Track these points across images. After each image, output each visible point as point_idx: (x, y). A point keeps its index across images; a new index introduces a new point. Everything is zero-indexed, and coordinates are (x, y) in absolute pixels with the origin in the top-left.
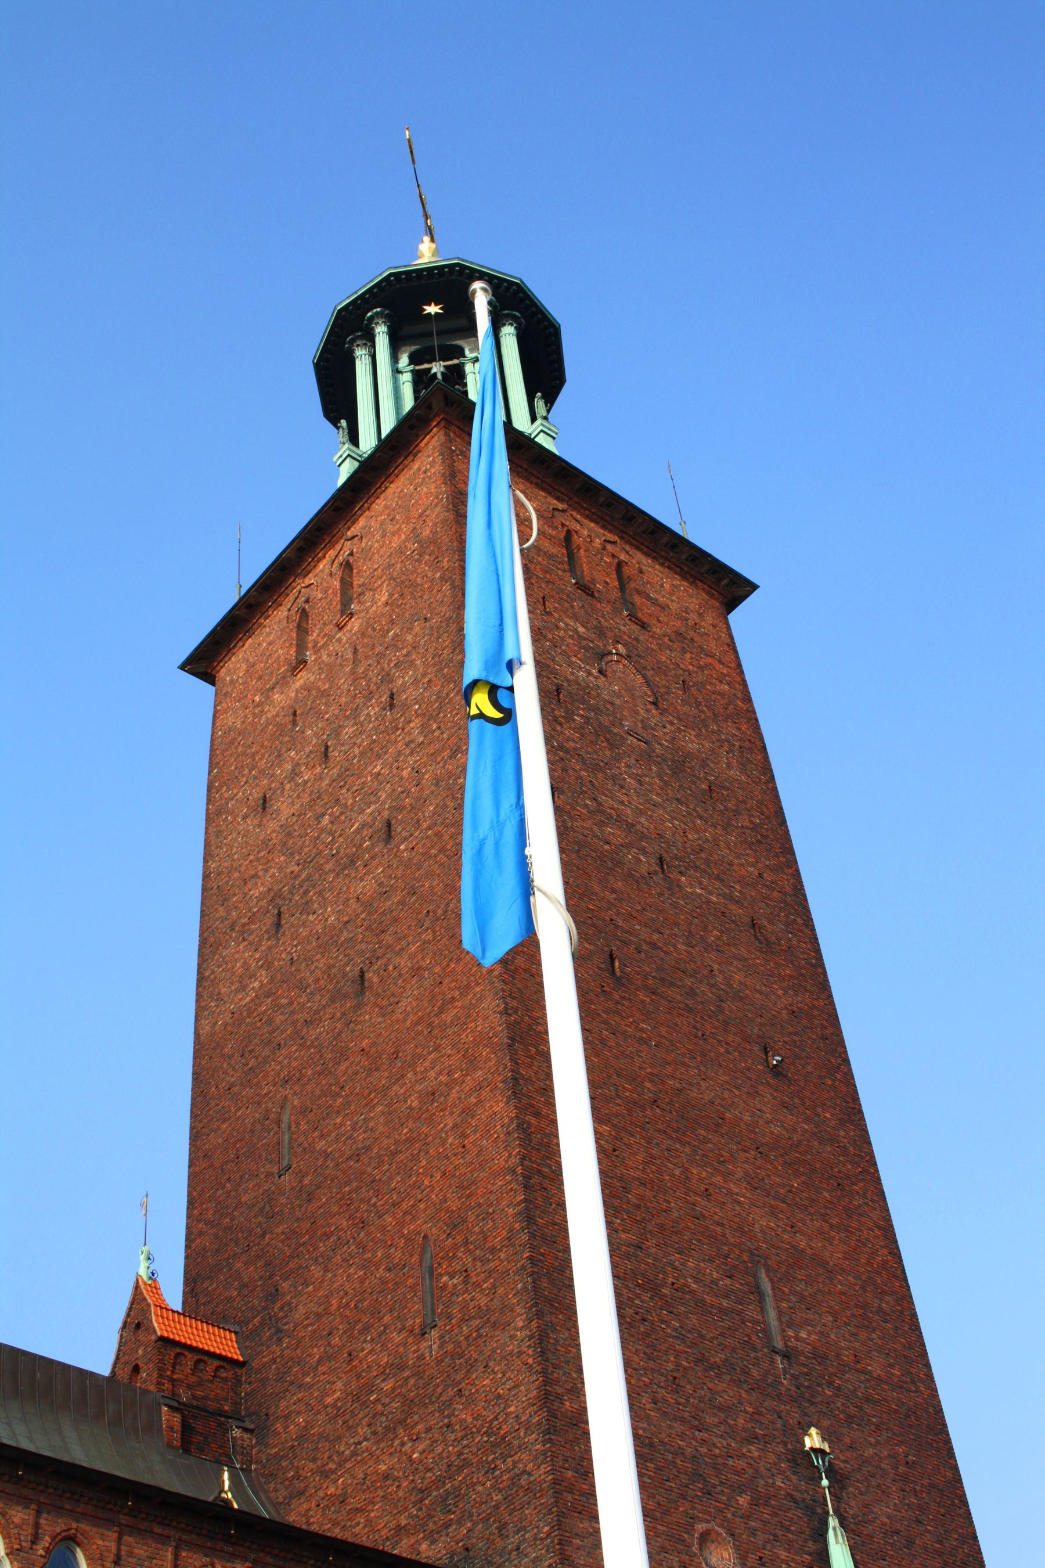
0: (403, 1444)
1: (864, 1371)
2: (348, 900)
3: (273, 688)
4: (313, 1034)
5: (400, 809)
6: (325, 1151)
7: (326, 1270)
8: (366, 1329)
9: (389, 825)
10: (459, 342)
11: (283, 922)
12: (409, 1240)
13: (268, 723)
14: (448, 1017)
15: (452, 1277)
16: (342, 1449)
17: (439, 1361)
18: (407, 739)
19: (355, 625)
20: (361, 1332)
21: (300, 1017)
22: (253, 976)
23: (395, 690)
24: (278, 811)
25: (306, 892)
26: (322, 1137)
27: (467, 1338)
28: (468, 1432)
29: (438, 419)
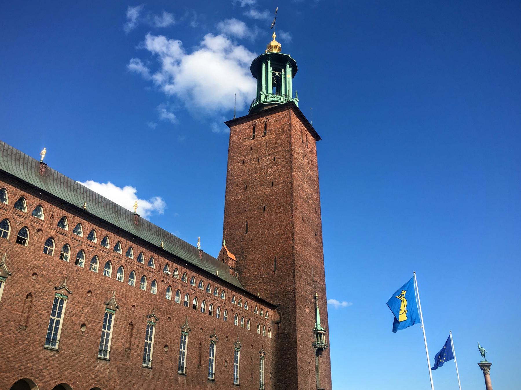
0: (269, 286)
1: (320, 283)
2: (262, 192)
7: (254, 253)
9: (272, 183)
16: (257, 282)
18: (277, 169)
19: (267, 138)
20: (261, 266)
27: (282, 275)
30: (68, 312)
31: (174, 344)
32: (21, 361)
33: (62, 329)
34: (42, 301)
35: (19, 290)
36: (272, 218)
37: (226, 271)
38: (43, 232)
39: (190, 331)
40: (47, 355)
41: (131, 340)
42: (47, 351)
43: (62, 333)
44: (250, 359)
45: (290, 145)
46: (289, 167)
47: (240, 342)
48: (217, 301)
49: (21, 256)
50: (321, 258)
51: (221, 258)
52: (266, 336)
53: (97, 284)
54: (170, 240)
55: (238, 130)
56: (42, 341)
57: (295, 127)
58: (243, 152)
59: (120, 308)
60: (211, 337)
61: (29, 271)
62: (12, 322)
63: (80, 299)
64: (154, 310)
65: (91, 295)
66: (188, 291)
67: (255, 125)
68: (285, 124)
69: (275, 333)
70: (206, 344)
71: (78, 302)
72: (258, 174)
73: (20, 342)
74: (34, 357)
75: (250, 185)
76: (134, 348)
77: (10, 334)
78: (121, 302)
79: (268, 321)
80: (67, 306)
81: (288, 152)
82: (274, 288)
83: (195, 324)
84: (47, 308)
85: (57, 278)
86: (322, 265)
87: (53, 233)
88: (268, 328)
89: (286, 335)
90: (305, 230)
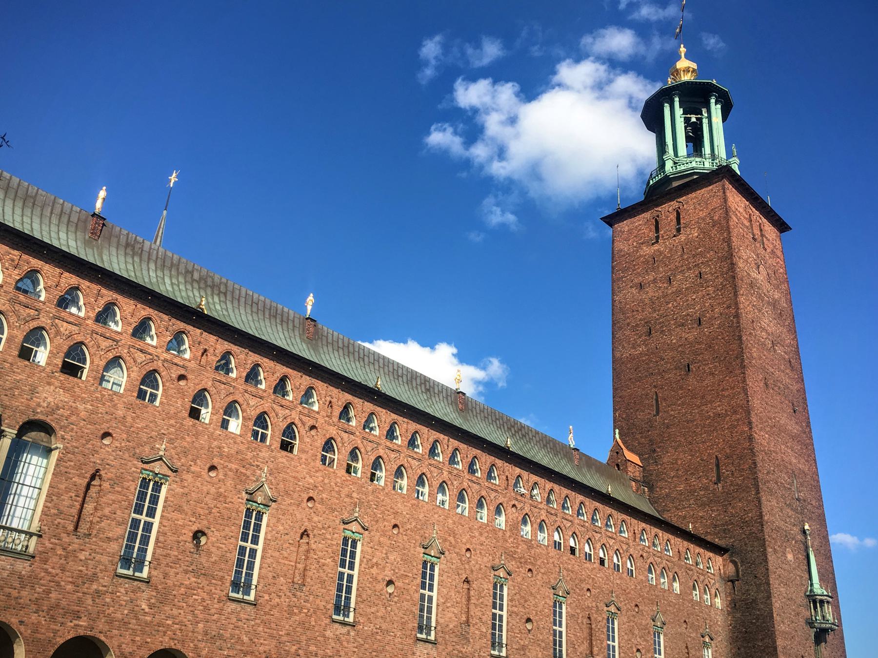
0: (708, 511)
1: (812, 504)
2: (681, 337)
4: (667, 376)
8: (692, 474)
13: (641, 256)
14: (726, 394)
15: (727, 471)
16: (684, 504)
17: (722, 493)
19: (682, 237)
20: (691, 474)
21: (662, 369)
22: (639, 346)
24: (648, 292)
25: (662, 327)
26: (672, 410)
30: (365, 560)
31: (541, 617)
32: (299, 642)
33: (358, 589)
34: (324, 542)
35: (289, 525)
36: (704, 384)
37: (623, 485)
38: (319, 430)
39: (569, 594)
40: (338, 633)
41: (468, 608)
42: (337, 625)
43: (358, 596)
44: (684, 647)
45: (730, 246)
46: (730, 286)
47: (663, 615)
48: (613, 541)
49: (288, 471)
50: (809, 456)
51: (613, 462)
52: (711, 606)
53: (407, 514)
54: (520, 433)
55: (626, 229)
56: (329, 609)
57: (737, 212)
58: (638, 268)
59: (447, 553)
60: (607, 606)
61: (302, 494)
62: (282, 578)
63: (381, 539)
64: (503, 558)
65: (399, 533)
66: (558, 524)
67: (658, 216)
68: (715, 208)
69: (729, 599)
70: (600, 619)
71: (380, 543)
72: (670, 305)
73: (295, 611)
74: (318, 636)
75: (658, 327)
76: (474, 622)
77: (280, 597)
78: (448, 543)
79: (712, 577)
80: (362, 551)
81: (726, 259)
82: (719, 515)
83: (577, 581)
84: (332, 555)
85: (345, 504)
86: (813, 469)
87: (333, 431)
88: (713, 591)
89: (751, 603)
90: (771, 403)
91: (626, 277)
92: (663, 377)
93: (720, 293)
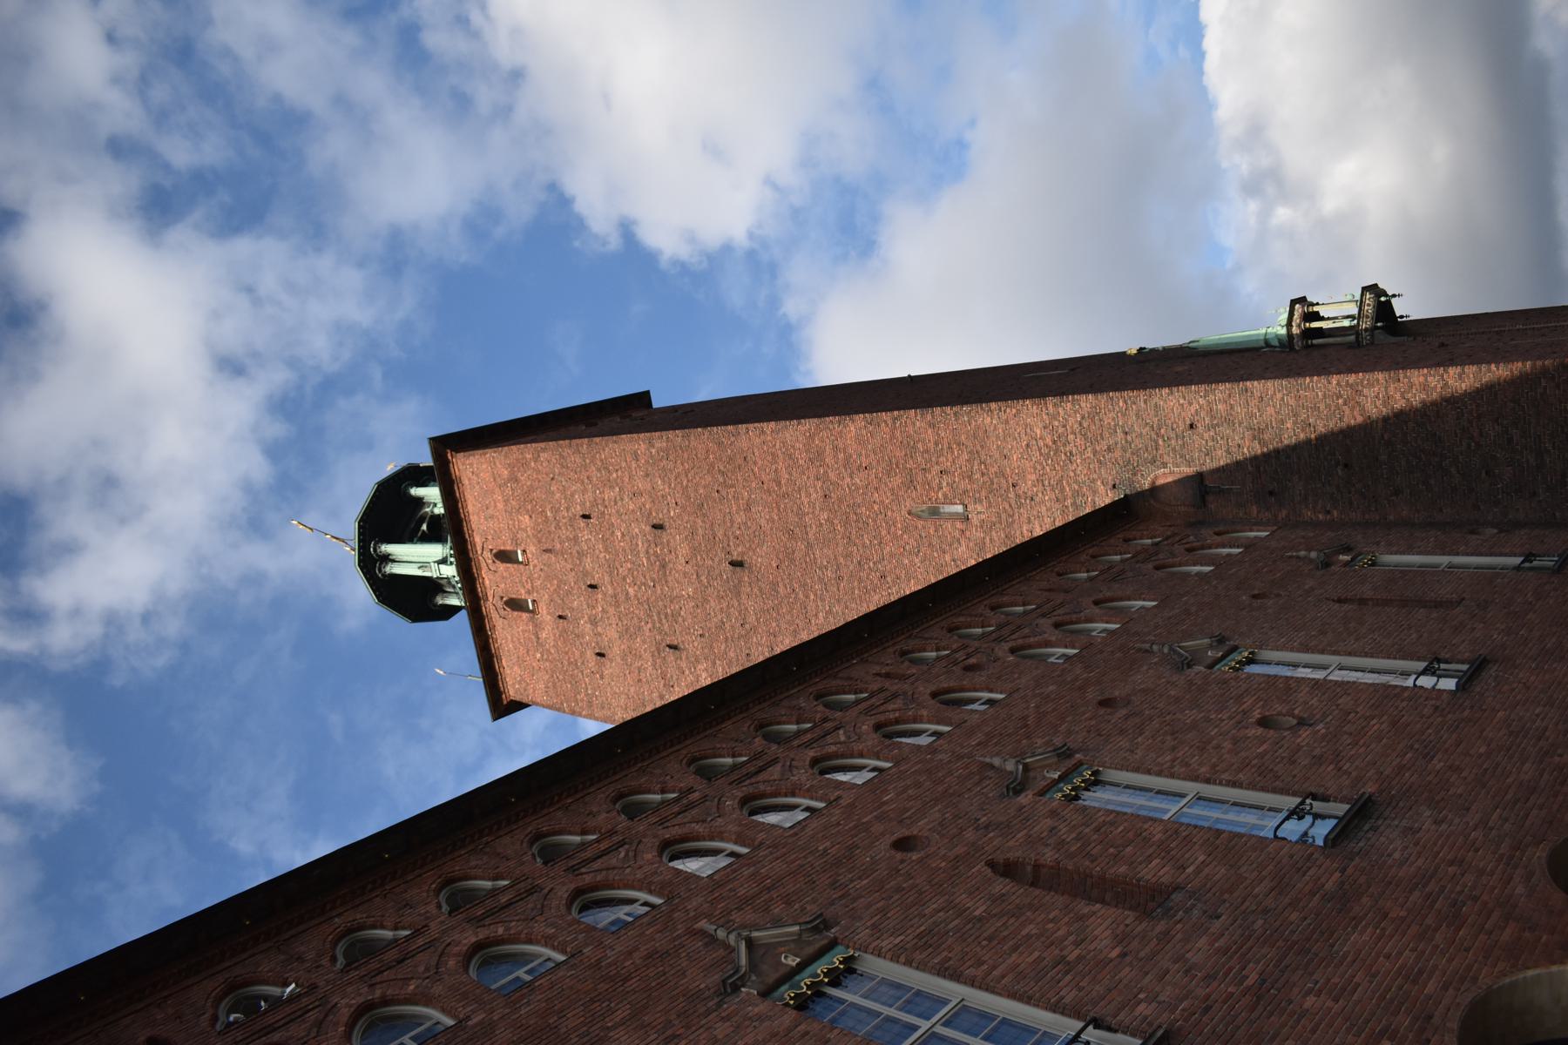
2: (685, 574)
3: (538, 638)
4: (752, 619)
5: (650, 513)
6: (826, 614)
9: (655, 527)
10: (422, 512)
11: (676, 643)
12: (906, 530)
18: (613, 503)
19: (532, 549)
23: (581, 513)
27: (983, 474)
28: (1040, 481)
29: (449, 455)
46: (604, 450)
48: (841, 732)
69: (1254, 509)
72: (631, 591)
91: (586, 684)
92: (754, 629)
93: (615, 475)
